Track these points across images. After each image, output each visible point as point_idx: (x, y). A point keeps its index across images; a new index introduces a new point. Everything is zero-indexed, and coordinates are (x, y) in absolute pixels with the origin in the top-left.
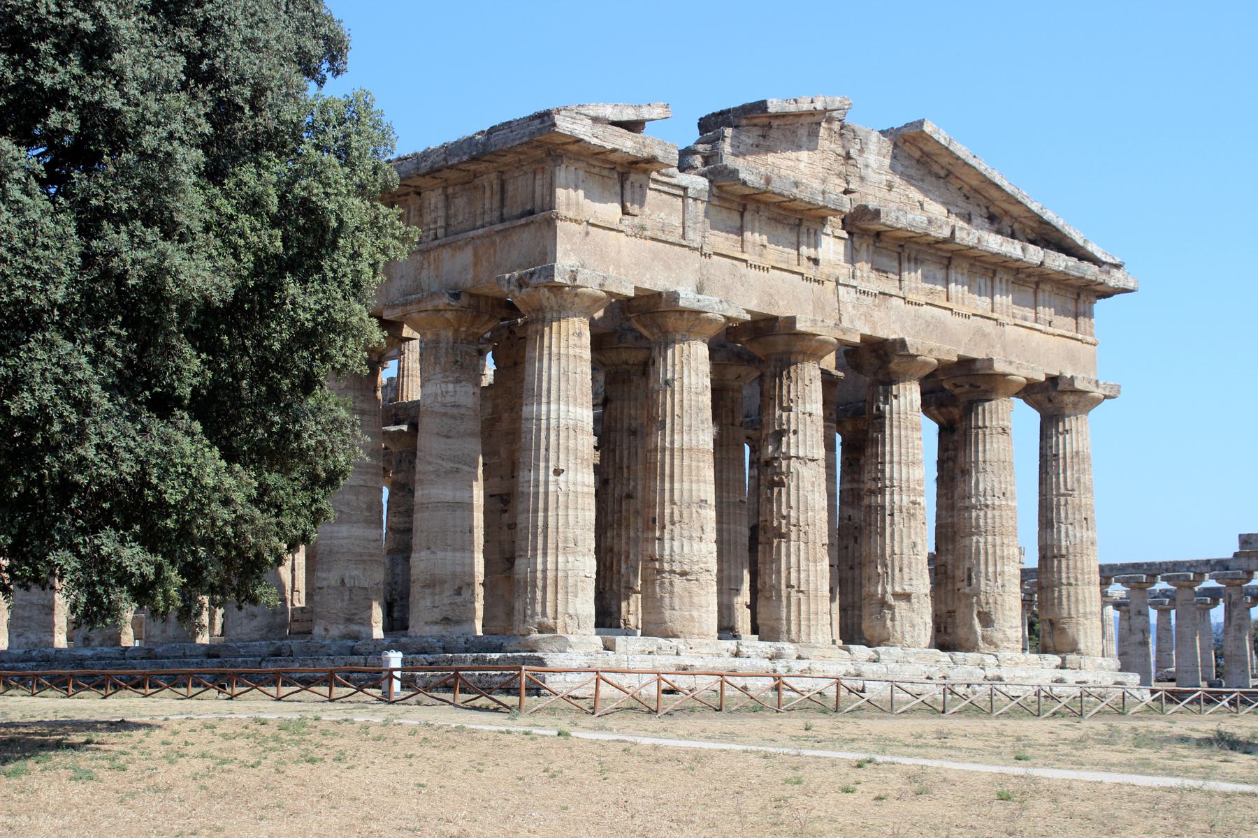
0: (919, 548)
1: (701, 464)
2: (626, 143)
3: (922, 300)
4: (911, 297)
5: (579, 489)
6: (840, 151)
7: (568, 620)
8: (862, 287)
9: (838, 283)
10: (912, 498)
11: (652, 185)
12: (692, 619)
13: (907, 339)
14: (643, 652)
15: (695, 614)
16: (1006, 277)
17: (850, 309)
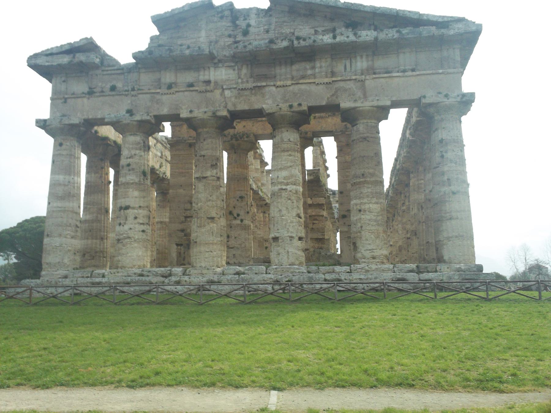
0: (284, 212)
1: (128, 190)
2: (65, 60)
3: (289, 83)
4: (279, 83)
5: (55, 209)
6: (229, 24)
7: (47, 266)
8: (241, 86)
9: (223, 90)
10: (280, 187)
11: (105, 73)
12: (119, 261)
13: (264, 106)
14: (83, 277)
15: (120, 258)
16: (365, 54)
17: (233, 99)
